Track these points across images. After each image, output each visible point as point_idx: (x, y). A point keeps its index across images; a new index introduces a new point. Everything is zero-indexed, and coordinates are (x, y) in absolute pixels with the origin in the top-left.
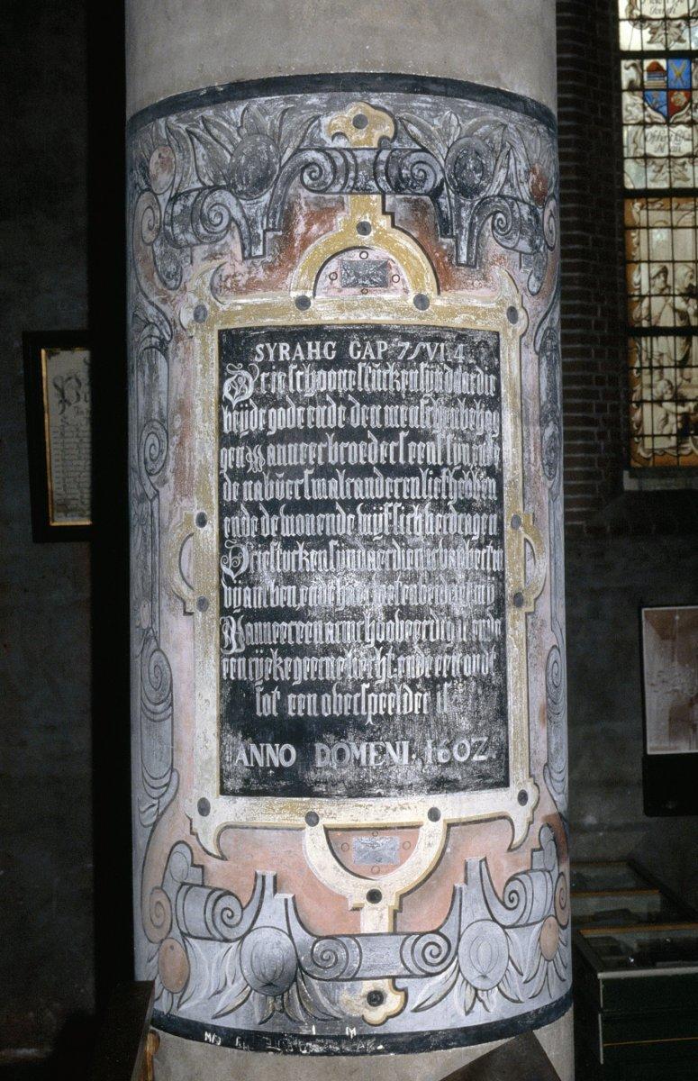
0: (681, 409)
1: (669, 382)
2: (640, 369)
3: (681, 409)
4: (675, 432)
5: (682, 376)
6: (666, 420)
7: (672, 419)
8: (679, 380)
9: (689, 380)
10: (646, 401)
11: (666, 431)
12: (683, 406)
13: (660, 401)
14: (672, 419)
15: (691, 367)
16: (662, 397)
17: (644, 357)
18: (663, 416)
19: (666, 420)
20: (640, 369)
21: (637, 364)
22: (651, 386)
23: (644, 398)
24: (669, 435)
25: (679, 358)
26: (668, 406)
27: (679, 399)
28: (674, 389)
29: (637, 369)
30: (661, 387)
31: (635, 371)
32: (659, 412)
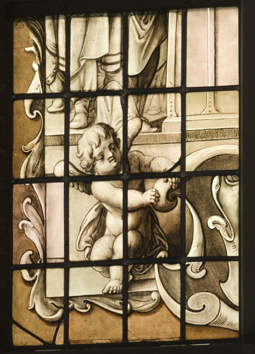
0: (135, 198)
1: (108, 129)
2: (39, 100)
3: (135, 198)
4: (119, 254)
5: (140, 115)
6: (99, 227)
7: (114, 222)
8: (133, 125)
9: (157, 124)
10: (54, 179)
11: (99, 252)
12: (142, 189)
13: (86, 180)
14: (114, 222)
15: (164, 90)
16: (92, 166)
17: (50, 70)
18: (92, 215)
19: (99, 227)
20: (39, 100)
21: (35, 87)
22: (66, 141)
23: (49, 170)
24: (106, 263)
25: (134, 68)
26: (108, 191)
27: (130, 173)
28: (120, 144)
29: (34, 97)
30: (88, 142)
31: (27, 103)
32: (83, 207)
